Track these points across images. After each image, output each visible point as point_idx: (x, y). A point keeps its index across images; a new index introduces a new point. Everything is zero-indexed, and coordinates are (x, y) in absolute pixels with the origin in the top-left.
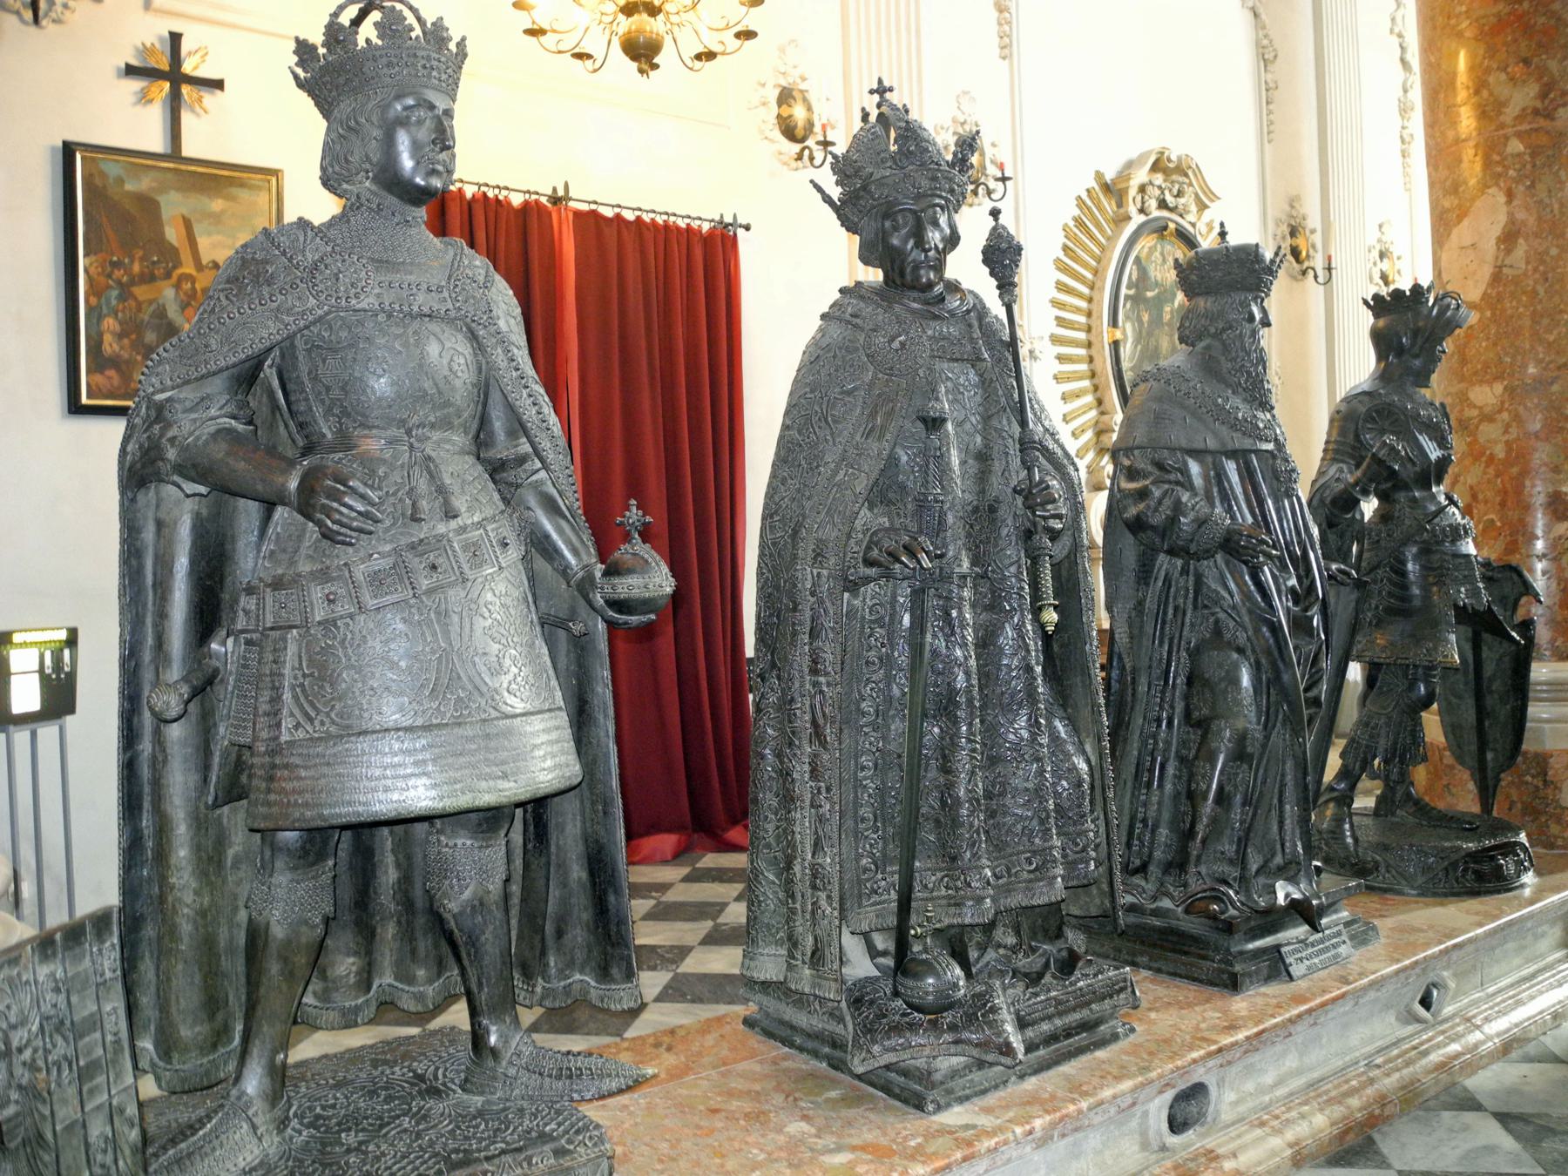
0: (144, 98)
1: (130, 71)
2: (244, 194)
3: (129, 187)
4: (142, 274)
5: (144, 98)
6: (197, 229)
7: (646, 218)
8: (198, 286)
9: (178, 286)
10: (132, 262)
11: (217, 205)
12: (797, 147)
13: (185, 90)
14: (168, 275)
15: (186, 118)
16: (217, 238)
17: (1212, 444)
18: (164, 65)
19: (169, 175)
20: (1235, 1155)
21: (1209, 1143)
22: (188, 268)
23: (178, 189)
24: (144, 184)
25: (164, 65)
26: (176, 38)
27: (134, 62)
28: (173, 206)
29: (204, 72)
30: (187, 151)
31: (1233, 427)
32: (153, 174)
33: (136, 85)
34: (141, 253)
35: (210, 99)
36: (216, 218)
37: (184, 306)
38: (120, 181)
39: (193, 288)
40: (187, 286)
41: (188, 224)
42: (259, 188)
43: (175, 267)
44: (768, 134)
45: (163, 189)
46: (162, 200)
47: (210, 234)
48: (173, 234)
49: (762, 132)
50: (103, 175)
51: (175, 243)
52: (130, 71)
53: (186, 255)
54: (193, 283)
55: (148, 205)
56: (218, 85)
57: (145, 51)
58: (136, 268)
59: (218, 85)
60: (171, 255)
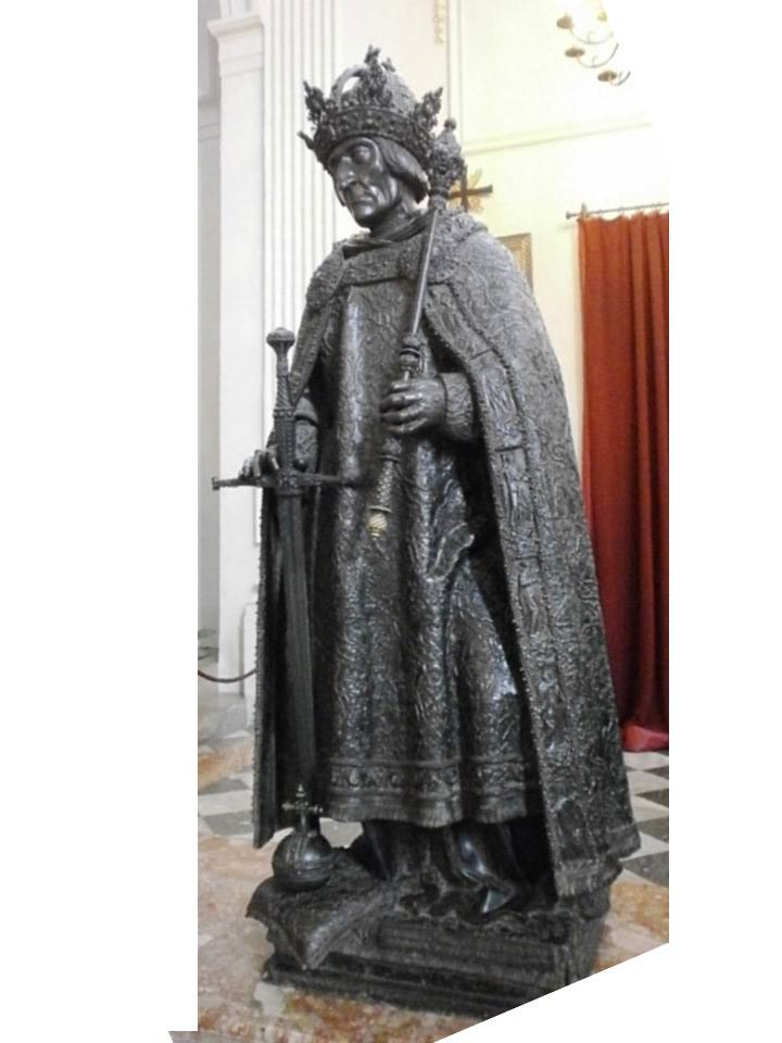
13: (470, 199)
35: (484, 201)
56: (488, 191)
59: (488, 191)
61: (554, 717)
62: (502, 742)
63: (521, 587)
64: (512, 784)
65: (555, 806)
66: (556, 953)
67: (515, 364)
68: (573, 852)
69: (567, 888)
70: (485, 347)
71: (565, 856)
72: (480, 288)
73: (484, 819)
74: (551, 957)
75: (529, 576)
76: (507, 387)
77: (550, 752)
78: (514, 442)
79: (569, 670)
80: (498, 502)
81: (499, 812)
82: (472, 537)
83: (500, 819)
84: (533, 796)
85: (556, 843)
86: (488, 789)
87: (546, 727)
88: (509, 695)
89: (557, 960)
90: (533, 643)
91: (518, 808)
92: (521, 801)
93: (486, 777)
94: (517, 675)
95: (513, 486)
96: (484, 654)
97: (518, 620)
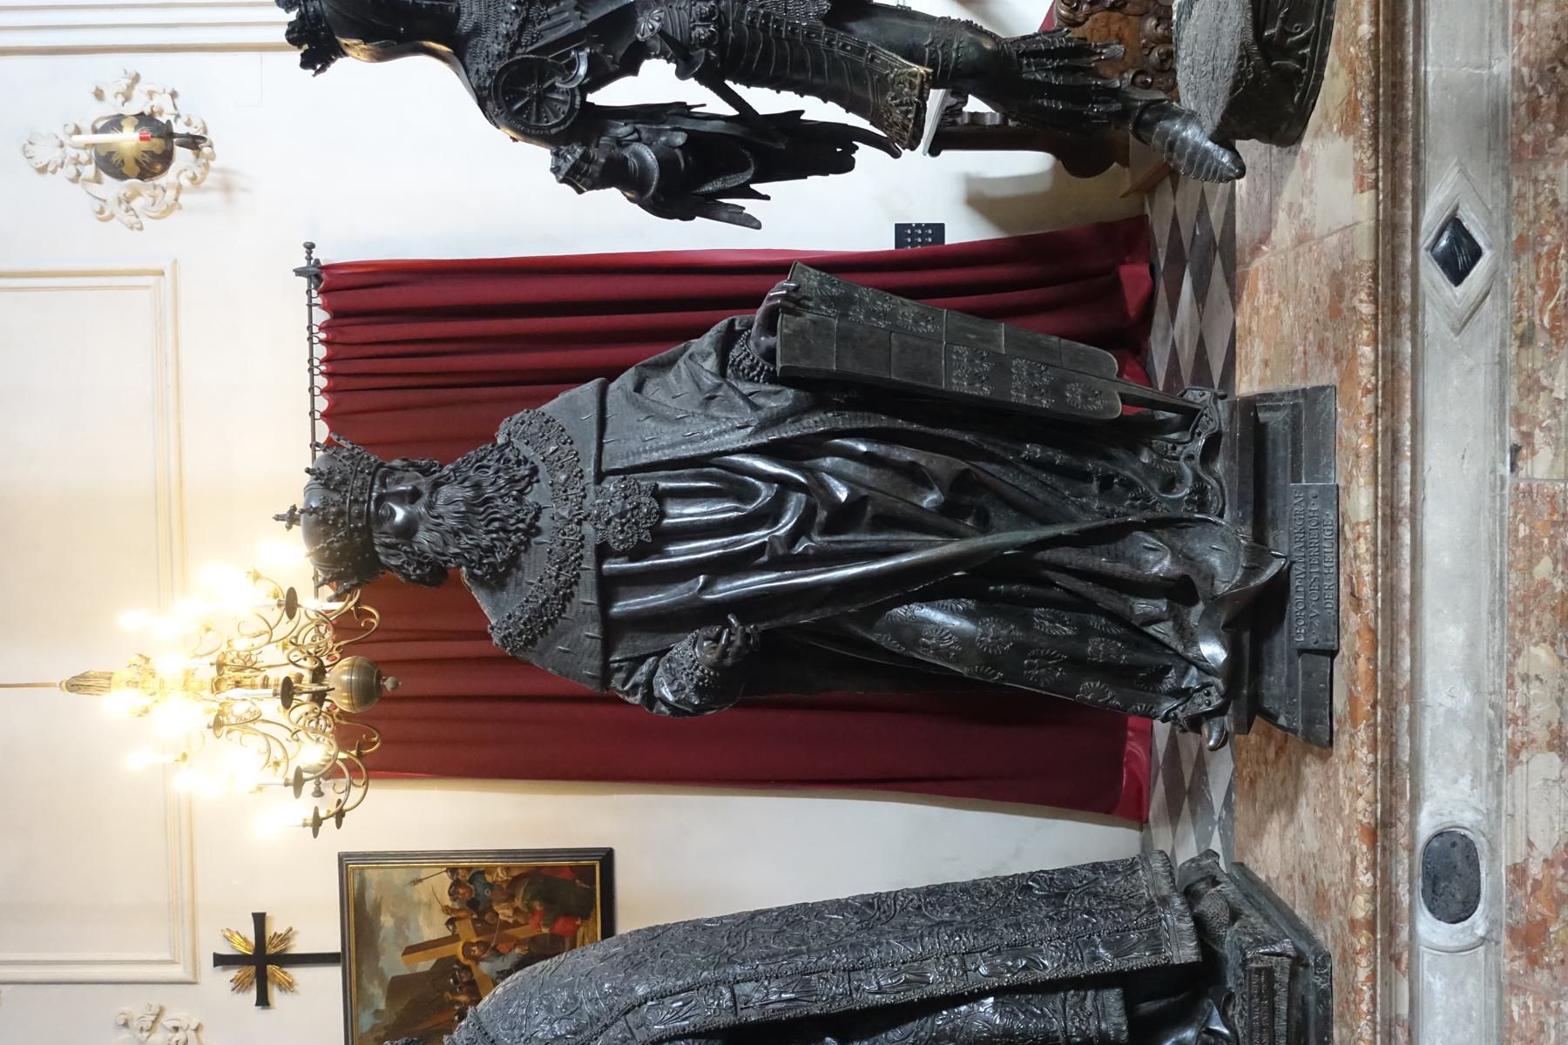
0: (287, 987)
1: (263, 1001)
2: (371, 895)
3: (382, 1006)
4: (469, 993)
5: (287, 987)
6: (415, 941)
7: (322, 404)
8: (475, 940)
9: (477, 960)
10: (458, 1002)
11: (387, 921)
12: (182, 155)
13: (271, 951)
14: (467, 968)
15: (298, 947)
16: (421, 920)
17: (594, 631)
18: (252, 969)
19: (364, 968)
20: (1530, 844)
21: (1505, 860)
22: (458, 949)
23: (377, 959)
24: (377, 995)
25: (252, 969)
26: (220, 961)
27: (253, 994)
28: (394, 964)
29: (250, 933)
30: (336, 947)
31: (568, 598)
32: (365, 981)
33: (274, 994)
34: (447, 994)
35: (274, 928)
36: (402, 923)
37: (497, 953)
38: (377, 1013)
39: (478, 944)
40: (476, 950)
41: (410, 950)
42: (363, 882)
43: (458, 962)
44: (171, 194)
45: (380, 974)
46: (389, 975)
47: (418, 929)
48: (424, 965)
49: (170, 209)
50: (373, 1029)
51: (432, 962)
52: (263, 1001)
53: (446, 951)
54: (473, 944)
55: (397, 987)
56: (260, 920)
57: (240, 986)
58: (463, 998)
59: (260, 920)
60: (446, 966)
61: (1014, 960)
62: (1044, 1015)
63: (880, 991)
64: (1089, 1003)
65: (1107, 960)
66: (1253, 965)
67: (641, 991)
68: (1155, 942)
69: (1189, 951)
70: (621, 1023)
71: (1157, 951)
72: (551, 1024)
73: (1124, 1037)
74: (1258, 971)
75: (870, 984)
76: (667, 1001)
77: (1050, 966)
78: (728, 996)
79: (964, 941)
80: (791, 1014)
81: (1116, 1020)
82: (828, 1039)
83: (1122, 1020)
84: (1100, 982)
85: (1141, 959)
86: (1092, 1032)
87: (1025, 968)
88: (994, 1005)
89: (1260, 965)
90: (938, 981)
91: (1113, 999)
92: (1106, 993)
93: (1081, 1033)
94: (976, 996)
95: (774, 998)
96: (953, 1030)
97: (914, 996)
